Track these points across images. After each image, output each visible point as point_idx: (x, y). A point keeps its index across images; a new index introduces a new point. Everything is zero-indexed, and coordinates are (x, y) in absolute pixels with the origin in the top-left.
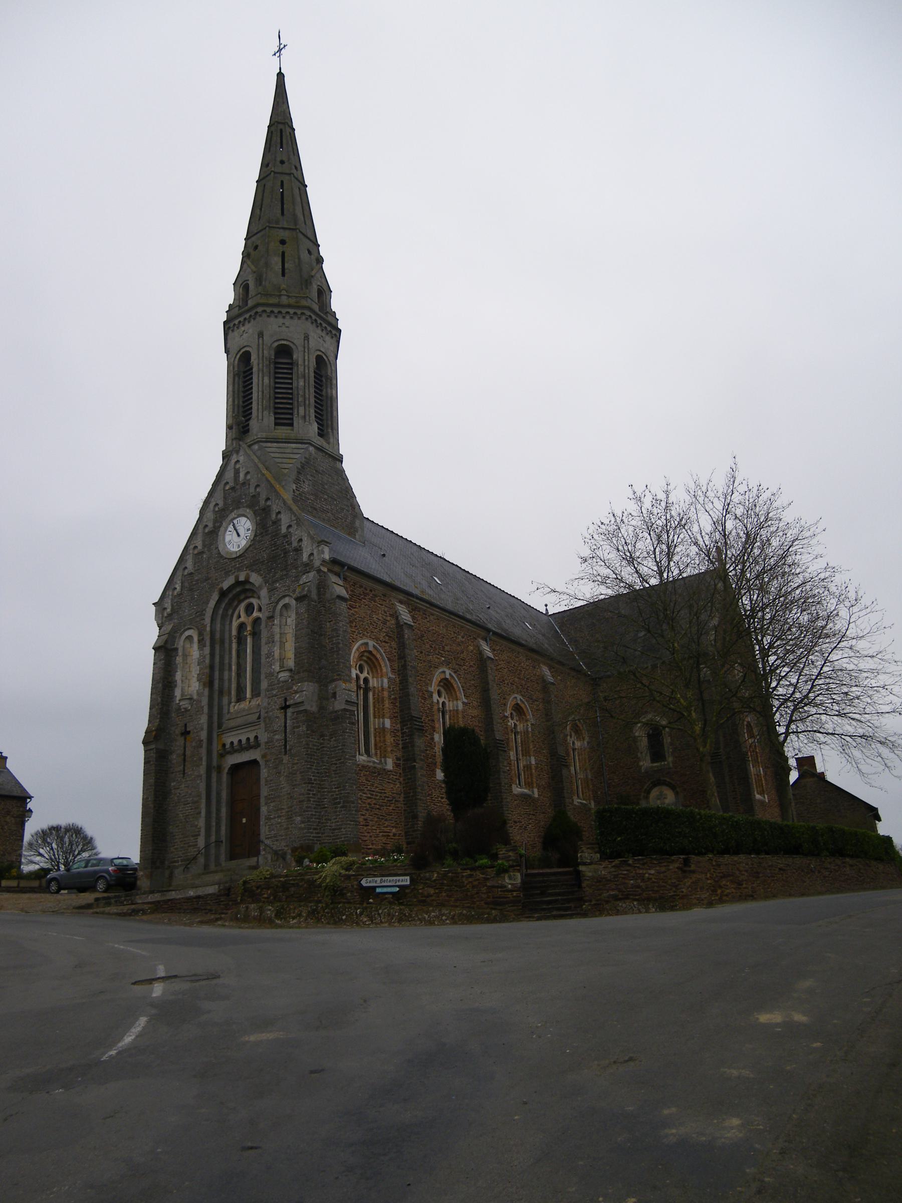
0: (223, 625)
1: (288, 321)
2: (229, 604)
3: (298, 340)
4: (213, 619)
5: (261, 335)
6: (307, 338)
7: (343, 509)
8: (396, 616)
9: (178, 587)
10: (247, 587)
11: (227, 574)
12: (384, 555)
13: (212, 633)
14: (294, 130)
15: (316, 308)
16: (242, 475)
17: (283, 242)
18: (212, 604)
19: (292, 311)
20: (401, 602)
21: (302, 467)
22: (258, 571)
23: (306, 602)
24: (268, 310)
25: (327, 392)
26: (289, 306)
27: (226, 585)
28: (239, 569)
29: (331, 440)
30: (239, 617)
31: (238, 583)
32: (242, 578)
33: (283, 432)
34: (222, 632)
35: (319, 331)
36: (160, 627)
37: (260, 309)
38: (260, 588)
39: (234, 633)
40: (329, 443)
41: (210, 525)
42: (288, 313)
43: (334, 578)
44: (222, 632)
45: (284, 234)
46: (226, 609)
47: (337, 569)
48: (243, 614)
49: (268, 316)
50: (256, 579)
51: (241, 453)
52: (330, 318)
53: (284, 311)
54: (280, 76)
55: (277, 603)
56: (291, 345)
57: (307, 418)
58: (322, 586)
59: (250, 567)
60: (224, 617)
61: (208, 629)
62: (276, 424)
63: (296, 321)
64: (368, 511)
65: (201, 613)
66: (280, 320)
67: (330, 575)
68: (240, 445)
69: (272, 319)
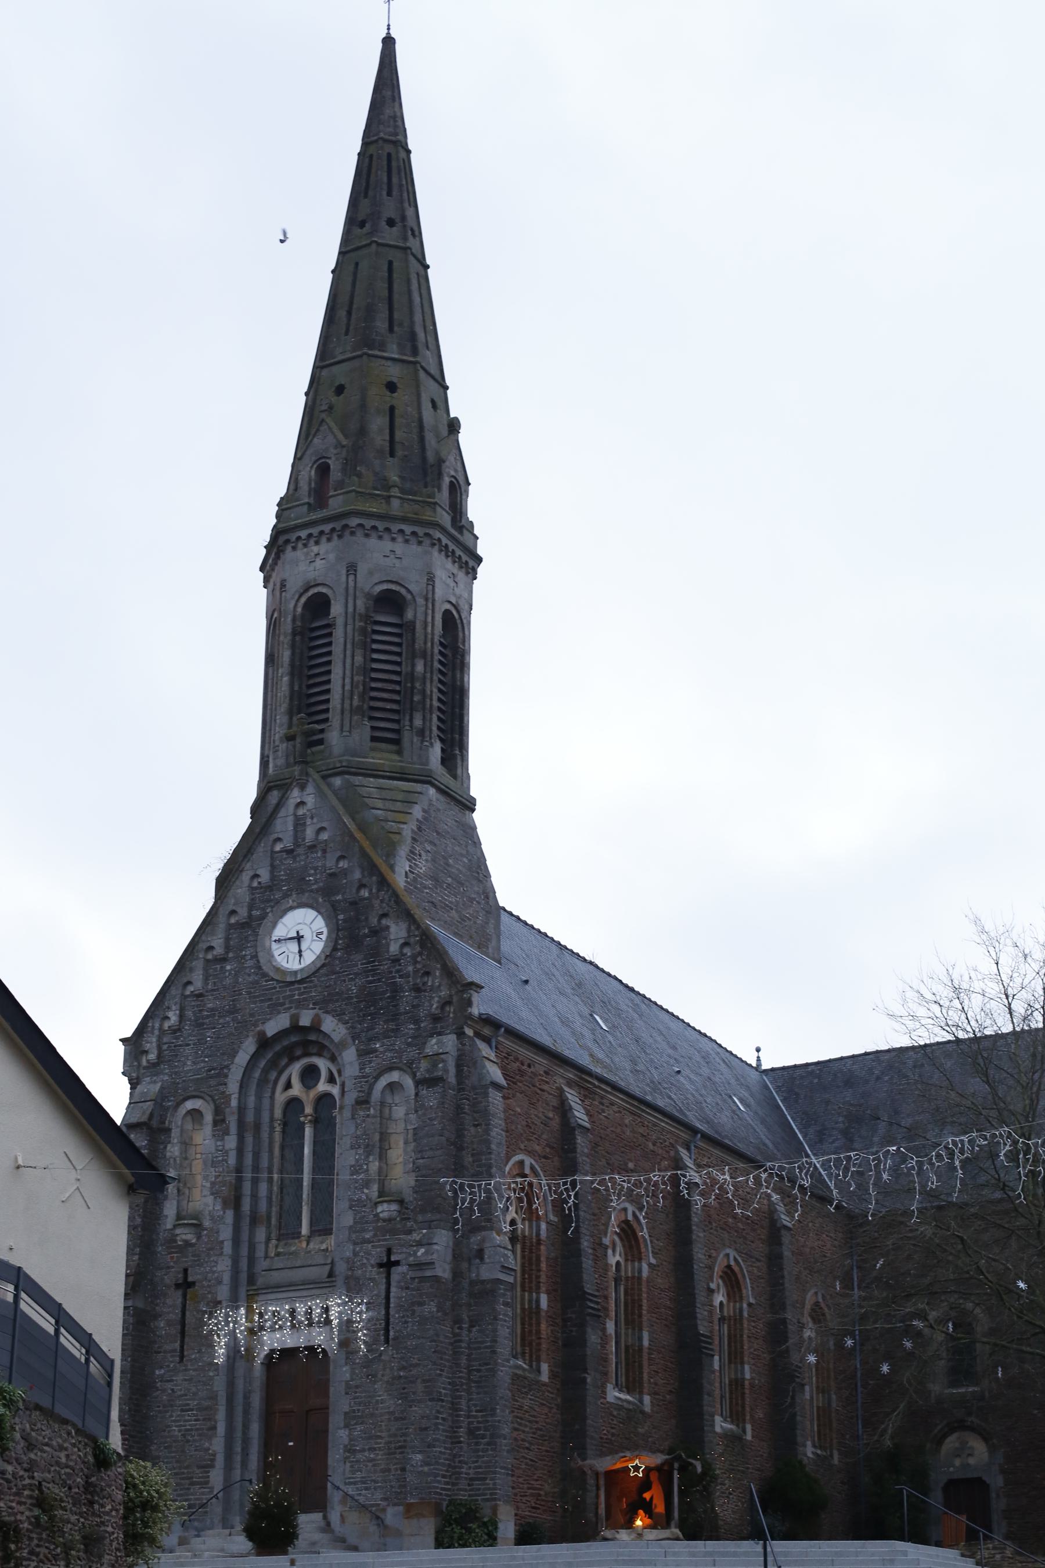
0: (259, 1098)
1: (399, 547)
2: (273, 1064)
3: (416, 585)
5: (352, 569)
6: (431, 579)
7: (471, 900)
8: (563, 1109)
9: (173, 1017)
10: (312, 1037)
11: (275, 1008)
12: (526, 982)
13: (242, 1110)
14: (409, 152)
15: (446, 519)
16: (310, 833)
17: (391, 387)
18: (242, 1058)
19: (408, 529)
20: (570, 1083)
21: (419, 829)
22: (339, 1015)
23: (438, 1089)
24: (368, 523)
25: (454, 676)
26: (404, 520)
27: (272, 1027)
28: (301, 1004)
29: (459, 771)
30: (288, 1086)
31: (295, 1028)
32: (305, 1021)
34: (258, 1110)
35: (449, 565)
36: (134, 1084)
37: (354, 522)
38: (342, 1045)
39: (278, 1113)
40: (455, 776)
41: (243, 912)
42: (401, 531)
43: (482, 1045)
44: (258, 1110)
45: (394, 372)
46: (265, 1071)
47: (487, 1031)
48: (296, 1081)
49: (367, 535)
50: (330, 1025)
51: (310, 789)
52: (466, 538)
53: (395, 527)
54: (389, 43)
55: (377, 1078)
56: (403, 591)
57: (427, 733)
58: (465, 1062)
59: (324, 1004)
61: (234, 1103)
62: (373, 739)
63: (414, 548)
64: (505, 899)
65: (221, 1074)
66: (387, 545)
67: (478, 1042)
68: (307, 774)
69: (373, 542)
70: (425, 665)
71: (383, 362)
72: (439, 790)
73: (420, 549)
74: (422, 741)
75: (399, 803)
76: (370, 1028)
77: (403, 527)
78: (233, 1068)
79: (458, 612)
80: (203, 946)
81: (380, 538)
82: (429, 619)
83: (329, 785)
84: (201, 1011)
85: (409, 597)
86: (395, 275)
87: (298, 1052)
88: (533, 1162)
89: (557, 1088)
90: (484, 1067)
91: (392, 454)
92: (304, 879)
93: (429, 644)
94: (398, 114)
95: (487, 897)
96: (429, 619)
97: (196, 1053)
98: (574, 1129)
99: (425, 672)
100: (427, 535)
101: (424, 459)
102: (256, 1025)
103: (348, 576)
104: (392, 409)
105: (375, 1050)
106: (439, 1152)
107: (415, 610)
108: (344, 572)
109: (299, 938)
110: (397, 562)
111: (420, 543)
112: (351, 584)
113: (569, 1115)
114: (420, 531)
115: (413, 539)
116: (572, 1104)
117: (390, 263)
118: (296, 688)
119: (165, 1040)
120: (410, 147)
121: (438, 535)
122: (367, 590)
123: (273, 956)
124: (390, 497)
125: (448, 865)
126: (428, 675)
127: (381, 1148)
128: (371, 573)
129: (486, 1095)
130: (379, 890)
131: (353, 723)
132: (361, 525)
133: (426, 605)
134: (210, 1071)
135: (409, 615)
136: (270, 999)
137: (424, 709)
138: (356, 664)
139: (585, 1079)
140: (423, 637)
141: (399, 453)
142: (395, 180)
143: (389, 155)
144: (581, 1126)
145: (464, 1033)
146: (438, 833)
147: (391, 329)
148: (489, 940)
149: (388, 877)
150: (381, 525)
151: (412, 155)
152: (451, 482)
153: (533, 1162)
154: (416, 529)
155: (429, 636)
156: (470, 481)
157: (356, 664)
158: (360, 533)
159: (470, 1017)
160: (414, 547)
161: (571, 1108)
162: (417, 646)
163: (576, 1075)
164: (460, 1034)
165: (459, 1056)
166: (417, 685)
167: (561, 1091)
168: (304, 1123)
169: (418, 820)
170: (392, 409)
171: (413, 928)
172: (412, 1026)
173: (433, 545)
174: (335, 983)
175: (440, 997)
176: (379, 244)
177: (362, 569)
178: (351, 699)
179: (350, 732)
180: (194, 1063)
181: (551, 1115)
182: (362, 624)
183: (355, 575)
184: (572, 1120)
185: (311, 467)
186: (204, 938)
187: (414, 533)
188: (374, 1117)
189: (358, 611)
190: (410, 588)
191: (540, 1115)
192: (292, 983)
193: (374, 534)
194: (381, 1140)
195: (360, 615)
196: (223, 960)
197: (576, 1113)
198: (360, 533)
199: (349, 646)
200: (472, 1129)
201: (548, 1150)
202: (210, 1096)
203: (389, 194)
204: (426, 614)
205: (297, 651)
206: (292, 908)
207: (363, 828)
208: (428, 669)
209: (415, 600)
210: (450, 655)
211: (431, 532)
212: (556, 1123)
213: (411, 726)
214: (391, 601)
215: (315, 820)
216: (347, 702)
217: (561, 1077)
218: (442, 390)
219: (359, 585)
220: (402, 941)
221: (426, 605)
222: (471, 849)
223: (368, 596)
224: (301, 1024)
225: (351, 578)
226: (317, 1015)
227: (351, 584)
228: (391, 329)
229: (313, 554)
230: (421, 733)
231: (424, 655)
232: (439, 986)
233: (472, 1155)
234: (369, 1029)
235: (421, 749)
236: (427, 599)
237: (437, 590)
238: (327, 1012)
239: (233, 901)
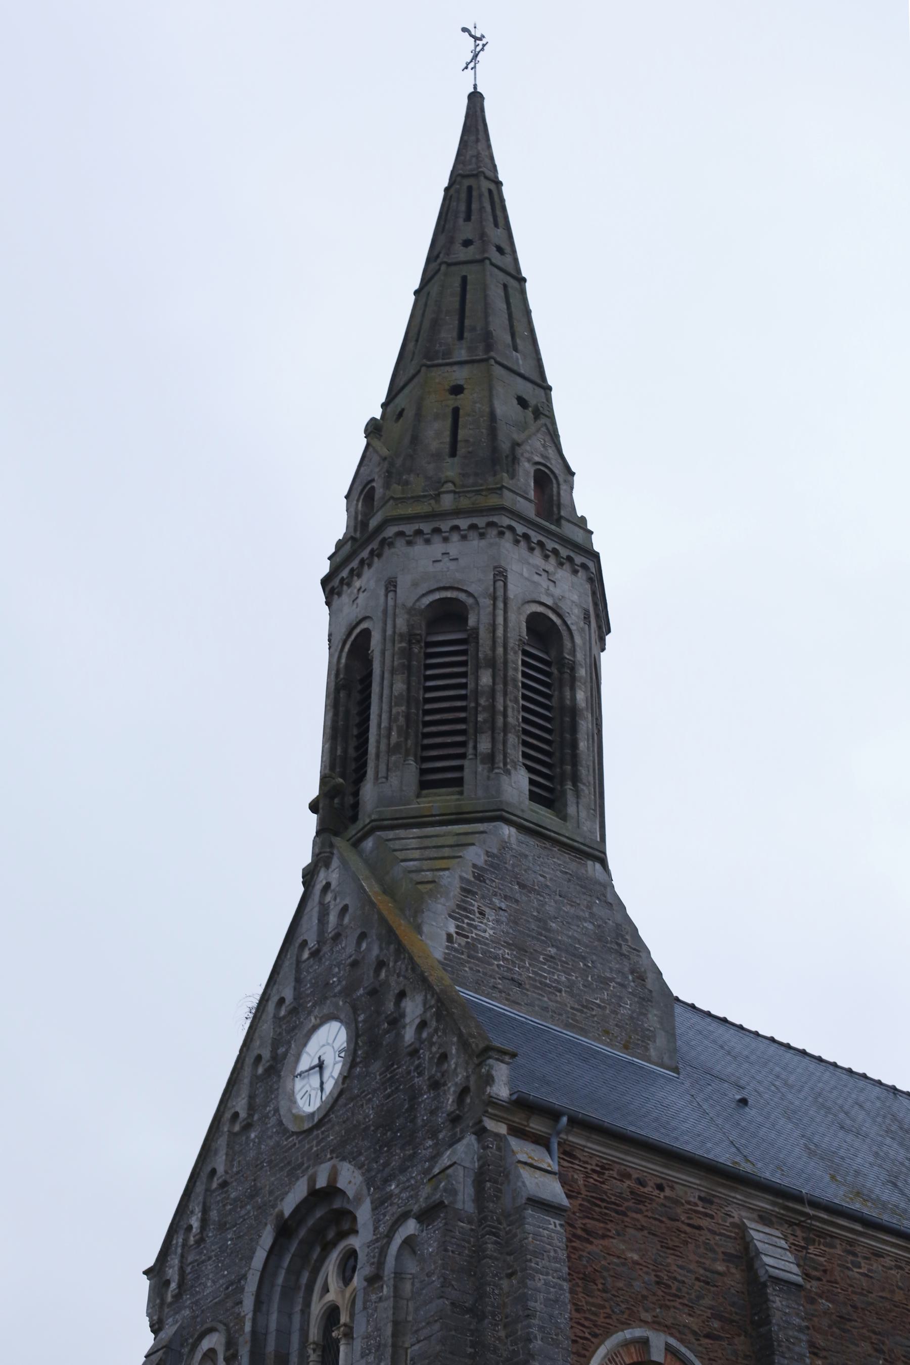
0: (286, 1313)
1: (455, 547)
2: (303, 1256)
3: (477, 582)
4: (259, 1303)
5: (391, 585)
6: (500, 575)
7: (605, 981)
8: (747, 1257)
9: (195, 1222)
10: (337, 1204)
11: (293, 1176)
12: (744, 1102)
13: (258, 1338)
14: (499, 184)
15: (529, 510)
16: (333, 918)
17: (457, 390)
18: (260, 1255)
19: (463, 523)
20: (764, 1219)
21: (479, 878)
22: (351, 1158)
23: (439, 1223)
24: (409, 529)
25: (562, 698)
26: (457, 513)
27: (288, 1206)
28: (318, 1159)
29: (571, 810)
30: (326, 1290)
31: (317, 1196)
32: (321, 1183)
33: (440, 801)
34: (284, 1333)
35: (537, 559)
36: (156, 1327)
37: (391, 531)
38: (358, 1200)
39: (314, 1333)
40: (564, 818)
41: (266, 1054)
42: (456, 528)
43: (523, 1150)
44: (284, 1333)
45: (460, 375)
46: (294, 1272)
47: (536, 1125)
48: (334, 1283)
49: (409, 543)
50: (350, 1178)
51: (335, 863)
52: (568, 530)
53: (445, 526)
54: (475, 100)
55: (390, 1236)
56: (462, 596)
57: (499, 757)
58: (491, 1176)
59: (340, 1152)
60: (288, 1293)
61: (248, 1327)
62: (424, 785)
63: (475, 543)
64: (681, 986)
65: (236, 1286)
66: (437, 548)
67: (514, 1143)
68: (332, 845)
69: (419, 548)
70: (494, 677)
71: (448, 368)
72: (520, 828)
73: (483, 543)
74: (492, 769)
75: (447, 849)
76: (386, 1164)
77: (457, 522)
78: (249, 1277)
79: (559, 615)
80: (228, 1115)
81: (428, 542)
82: (500, 620)
83: (360, 853)
84: (224, 1206)
85: (470, 601)
86: (468, 287)
87: (331, 1235)
88: (672, 1341)
89: (734, 1225)
90: (519, 1176)
91: (453, 453)
92: (328, 984)
93: (500, 650)
94: (484, 153)
95: (641, 978)
96: (500, 620)
97: (217, 1266)
98: (764, 1285)
99: (494, 683)
100: (491, 524)
101: (495, 449)
102: (274, 1207)
103: (386, 596)
104: (456, 412)
105: (391, 1195)
106: (437, 1326)
107: (479, 614)
108: (382, 592)
109: (321, 1066)
110: (452, 566)
111: (482, 536)
112: (391, 602)
113: (757, 1265)
114: (481, 522)
115: (473, 535)
116: (759, 1245)
117: (464, 280)
118: (339, 752)
119: (190, 1259)
120: (501, 178)
121: (506, 521)
122: (409, 604)
123: (295, 1102)
124: (438, 495)
125: (549, 930)
126: (500, 687)
127: (394, 1345)
128: (415, 584)
129: (521, 1221)
130: (396, 962)
131: (391, 765)
132: (401, 534)
133: (494, 605)
134: (227, 1288)
135: (472, 622)
136: (289, 1163)
137: (493, 729)
138: (396, 693)
139: (792, 1208)
140: (489, 642)
141: (462, 450)
142: (475, 206)
143: (470, 189)
144: (777, 1280)
145: (484, 1129)
146: (522, 886)
147: (461, 337)
148: (653, 1038)
149: (406, 942)
150: (426, 527)
151: (504, 189)
152: (537, 472)
153: (672, 1341)
154: (475, 520)
155: (500, 641)
156: (573, 470)
157: (396, 693)
158: (400, 543)
159: (492, 1102)
160: (475, 542)
161: (758, 1253)
162: (481, 655)
163: (774, 1204)
164: (481, 1132)
165: (481, 1167)
166: (483, 701)
167: (742, 1229)
168: (338, 1341)
169: (474, 866)
170: (456, 412)
171: (429, 997)
172: (430, 1143)
173: (501, 534)
174: (353, 1114)
175: (456, 1084)
176: (449, 265)
177: (404, 582)
178: (389, 736)
179: (387, 778)
180: (214, 1282)
181: (720, 1267)
182: (404, 645)
183: (395, 591)
184: (761, 1272)
185: (358, 500)
186: (229, 1105)
187: (473, 527)
188: (387, 1298)
189: (397, 631)
190: (469, 589)
191: (693, 1266)
192: (310, 1131)
193: (419, 540)
194: (395, 1335)
195: (401, 635)
196: (247, 1127)
197: (766, 1260)
198: (400, 543)
199: (387, 675)
200: (505, 1283)
201: (716, 1324)
202: (225, 1325)
203: (468, 218)
204: (494, 616)
205: (342, 709)
206: (315, 1028)
207: (389, 890)
208: (499, 680)
209: (477, 603)
210: (555, 672)
211: (495, 519)
212: (734, 1279)
213: (476, 755)
214: (448, 612)
215: (338, 900)
216: (384, 742)
217: (740, 1210)
218: (542, 392)
219: (399, 601)
220: (417, 1021)
221: (494, 605)
222: (599, 910)
223: (411, 611)
224: (318, 1186)
225: (391, 595)
226: (334, 1167)
227: (391, 602)
228: (461, 337)
229: (356, 591)
230: (490, 759)
231: (492, 663)
232: (455, 1069)
233: (505, 1326)
234: (386, 1164)
235: (488, 778)
236: (495, 599)
237: (510, 586)
238: (344, 1159)
239: (258, 1043)
